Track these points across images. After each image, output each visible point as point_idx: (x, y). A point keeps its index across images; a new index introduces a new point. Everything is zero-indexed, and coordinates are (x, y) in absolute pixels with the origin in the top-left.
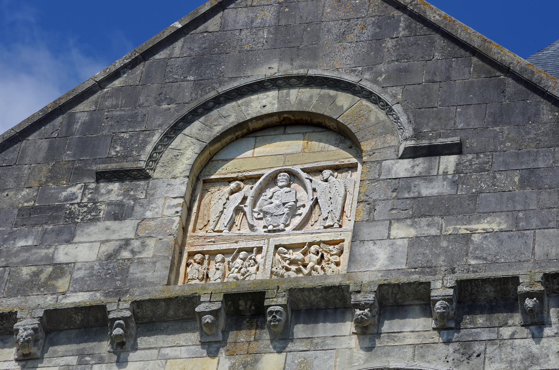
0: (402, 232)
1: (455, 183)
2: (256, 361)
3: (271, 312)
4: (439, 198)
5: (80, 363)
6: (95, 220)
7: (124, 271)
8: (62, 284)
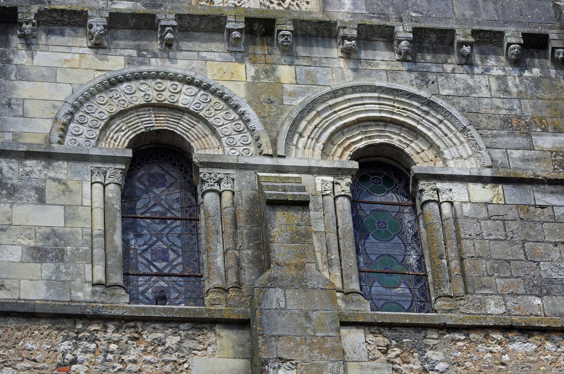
2: (274, 70)
3: (283, 35)
5: (139, 55)
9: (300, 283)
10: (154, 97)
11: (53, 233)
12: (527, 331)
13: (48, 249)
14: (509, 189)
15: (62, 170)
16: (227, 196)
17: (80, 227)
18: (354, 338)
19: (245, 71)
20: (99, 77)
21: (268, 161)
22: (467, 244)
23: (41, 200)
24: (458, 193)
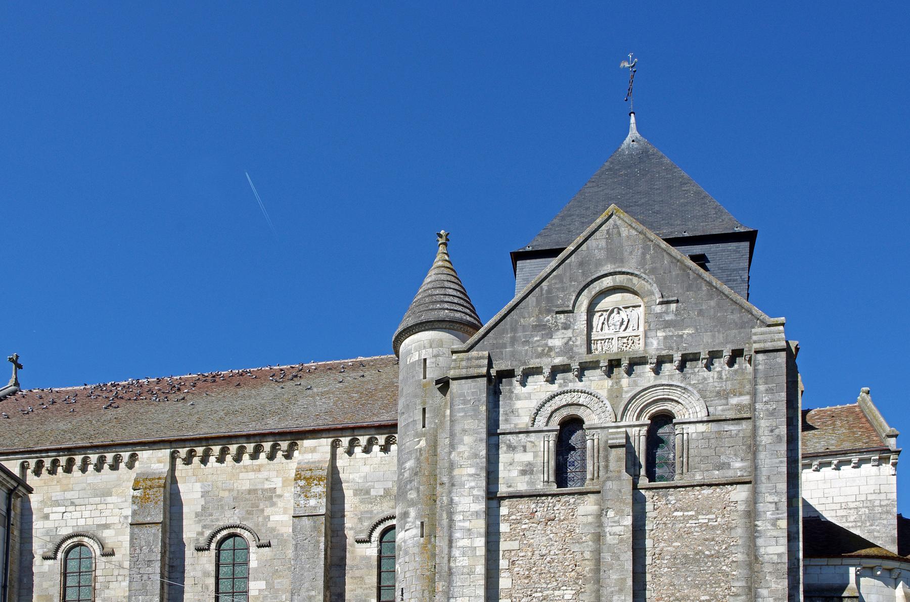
0: (661, 334)
1: (676, 315)
4: (672, 321)
6: (558, 329)
7: (572, 349)
8: (552, 354)
11: (529, 464)
14: (713, 424)
15: (533, 437)
16: (596, 441)
20: (548, 395)
21: (614, 424)
22: (691, 451)
23: (525, 451)
24: (691, 429)
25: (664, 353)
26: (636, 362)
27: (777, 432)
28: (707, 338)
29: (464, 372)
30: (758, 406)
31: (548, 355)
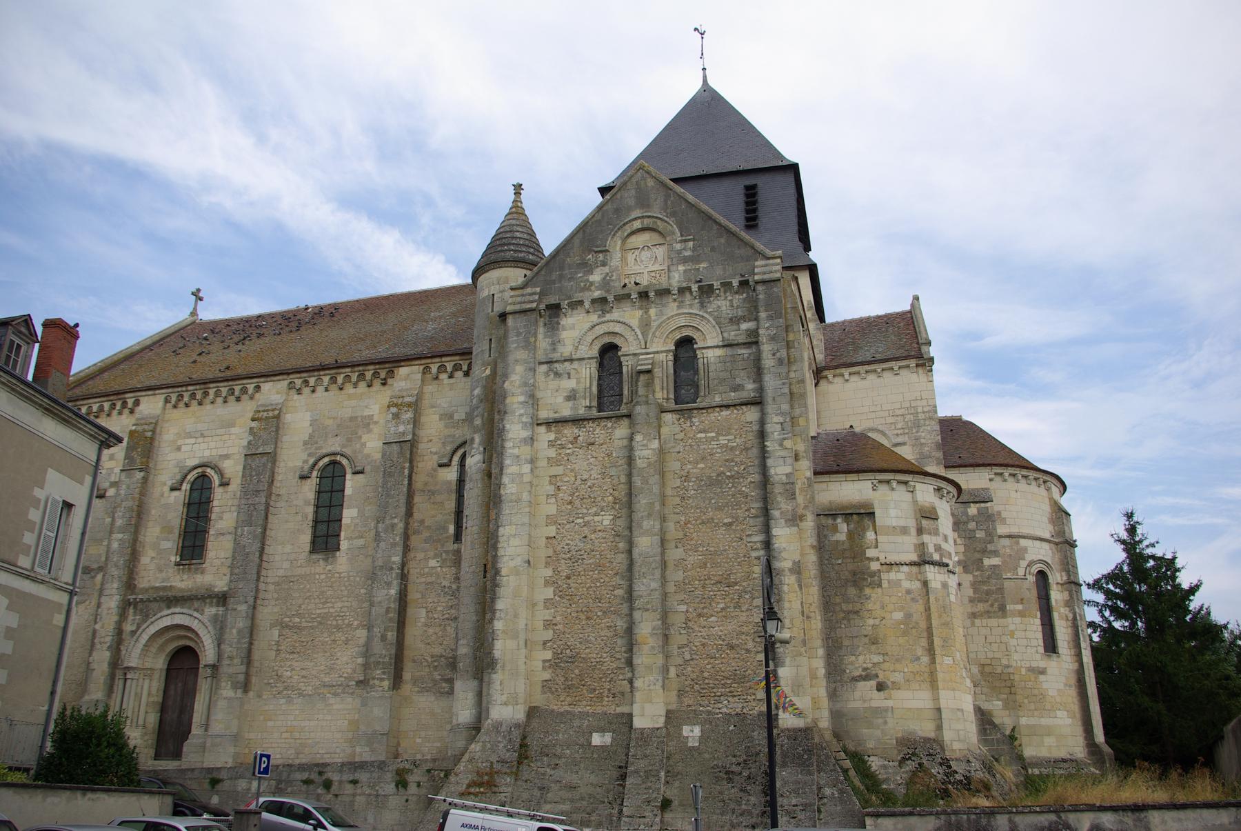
0: (681, 268)
9: (647, 403)
10: (607, 330)
12: (728, 406)
13: (572, 397)
15: (576, 365)
17: (582, 386)
18: (668, 417)
19: (639, 313)
20: (588, 325)
24: (710, 354)
25: (684, 285)
26: (664, 293)
27: (778, 355)
28: (719, 271)
29: (517, 307)
30: (761, 332)
31: (589, 289)
